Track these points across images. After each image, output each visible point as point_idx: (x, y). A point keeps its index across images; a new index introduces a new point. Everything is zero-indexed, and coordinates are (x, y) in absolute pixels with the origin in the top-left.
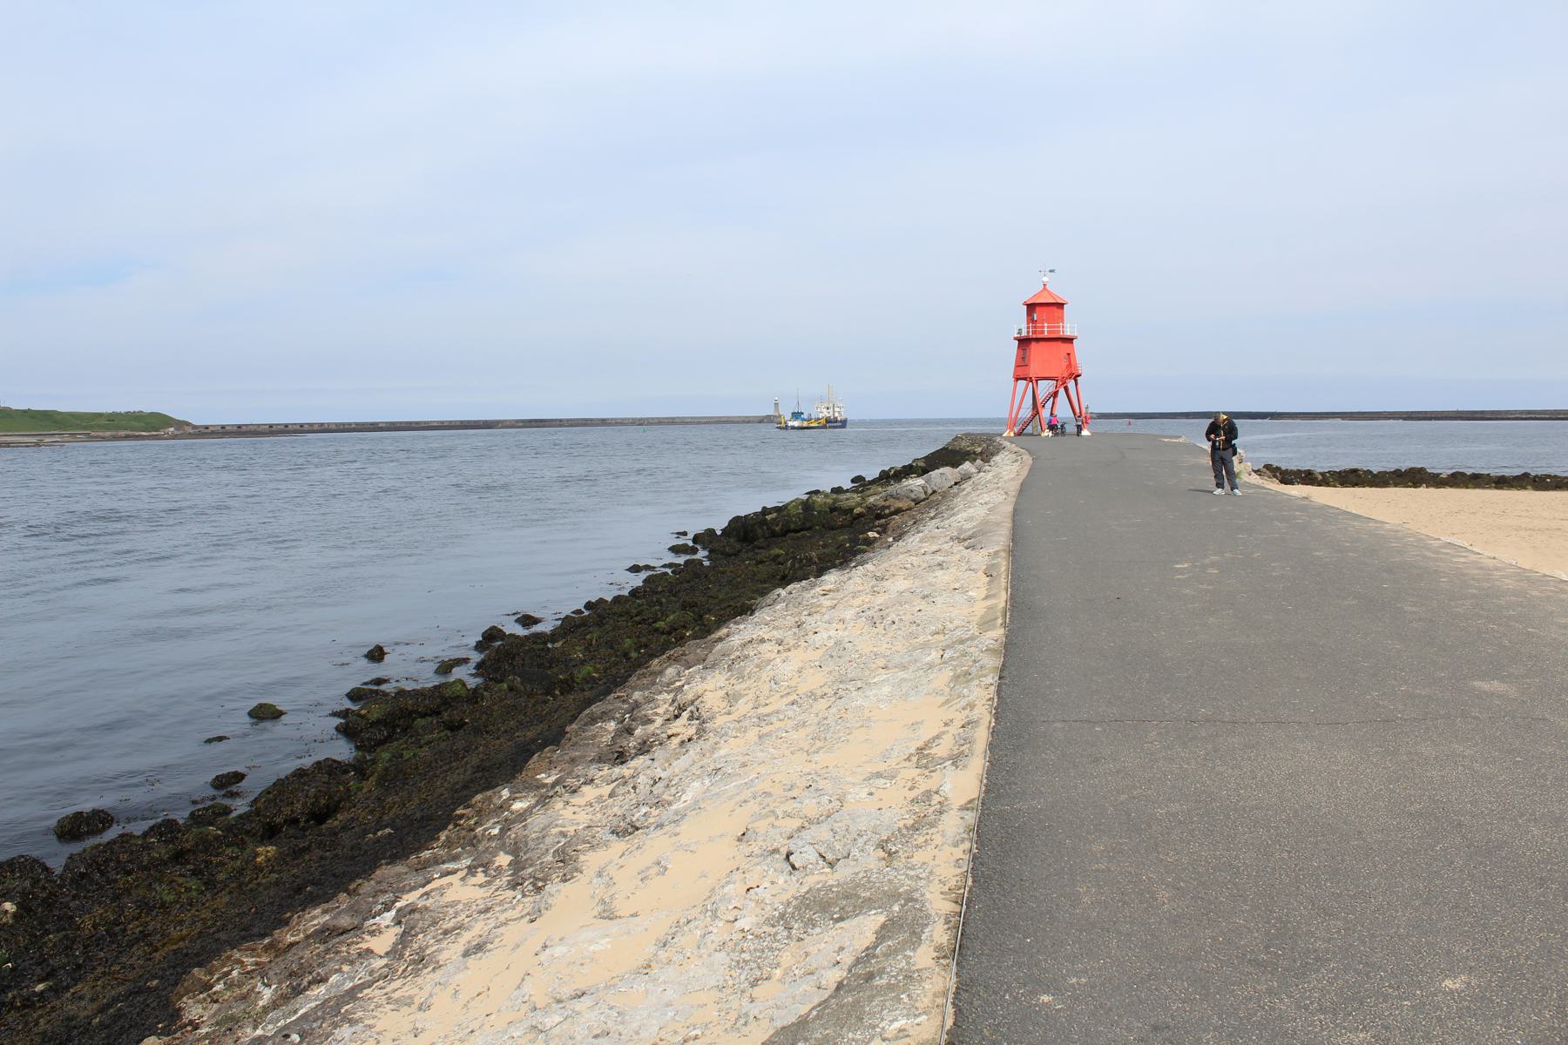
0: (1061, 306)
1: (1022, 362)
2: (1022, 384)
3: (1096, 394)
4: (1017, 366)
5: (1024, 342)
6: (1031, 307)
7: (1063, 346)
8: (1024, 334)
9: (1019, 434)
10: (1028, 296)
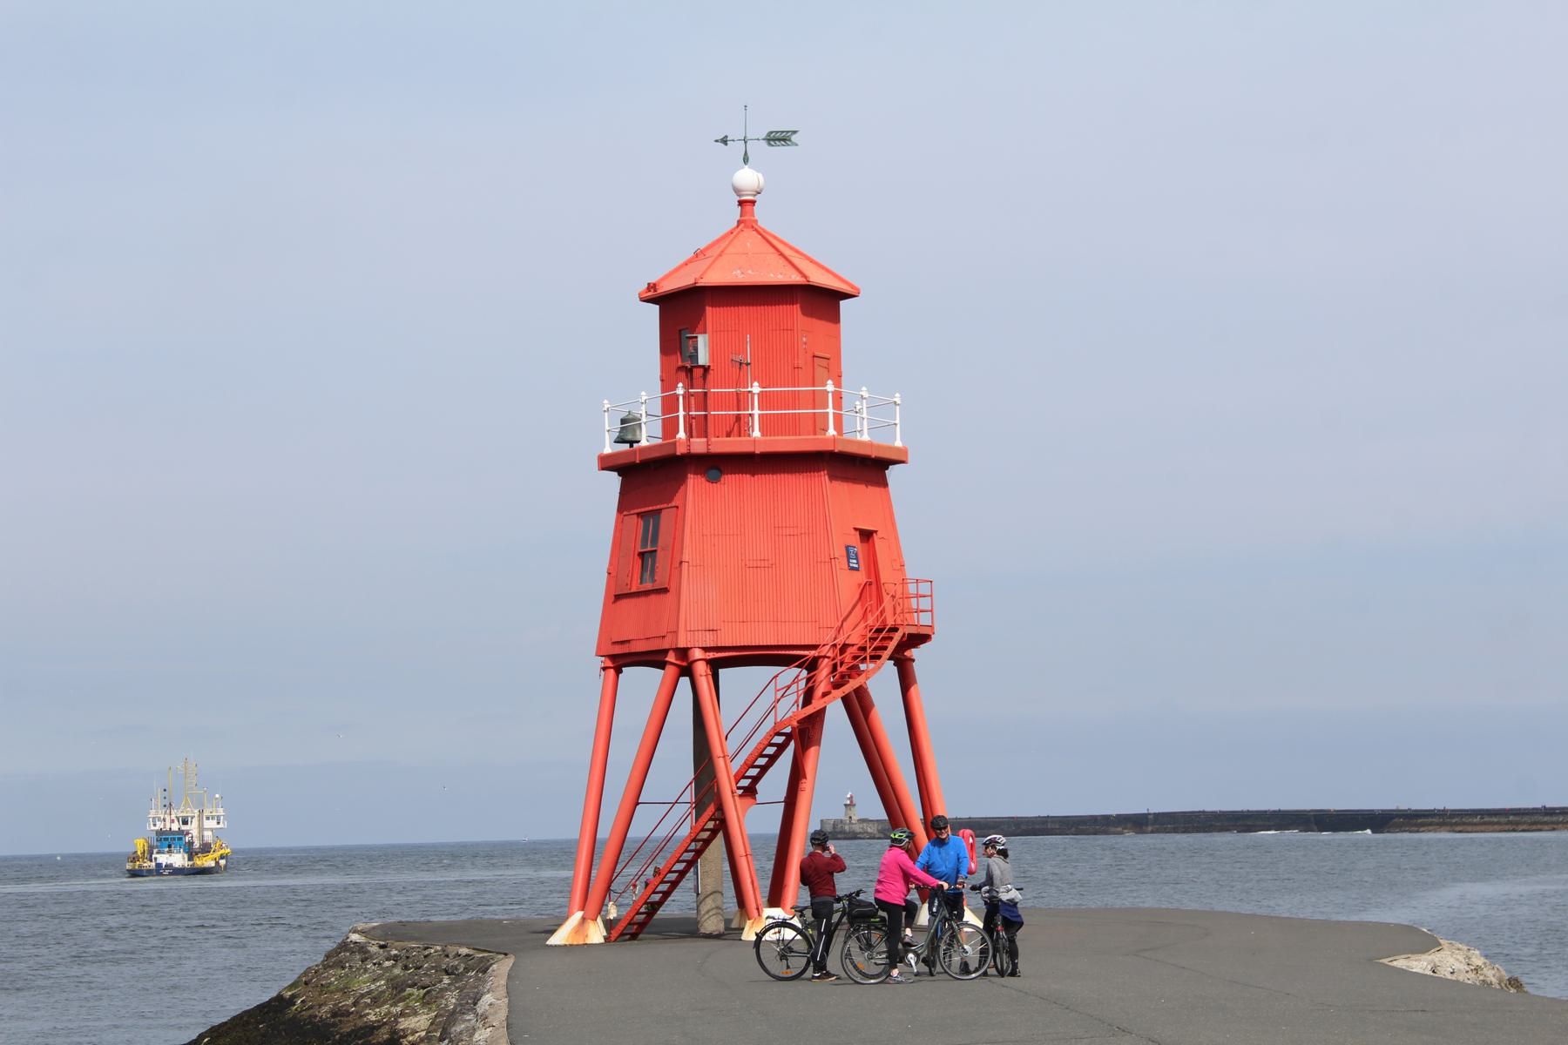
0: (823, 301)
1: (641, 574)
2: (642, 683)
3: (1002, 723)
4: (617, 596)
5: (647, 478)
6: (681, 309)
7: (844, 502)
8: (649, 436)
9: (636, 929)
10: (668, 263)
